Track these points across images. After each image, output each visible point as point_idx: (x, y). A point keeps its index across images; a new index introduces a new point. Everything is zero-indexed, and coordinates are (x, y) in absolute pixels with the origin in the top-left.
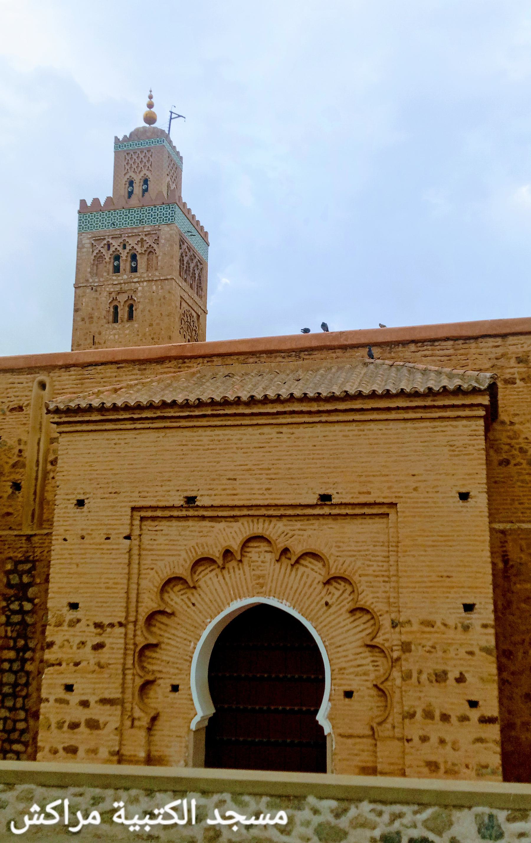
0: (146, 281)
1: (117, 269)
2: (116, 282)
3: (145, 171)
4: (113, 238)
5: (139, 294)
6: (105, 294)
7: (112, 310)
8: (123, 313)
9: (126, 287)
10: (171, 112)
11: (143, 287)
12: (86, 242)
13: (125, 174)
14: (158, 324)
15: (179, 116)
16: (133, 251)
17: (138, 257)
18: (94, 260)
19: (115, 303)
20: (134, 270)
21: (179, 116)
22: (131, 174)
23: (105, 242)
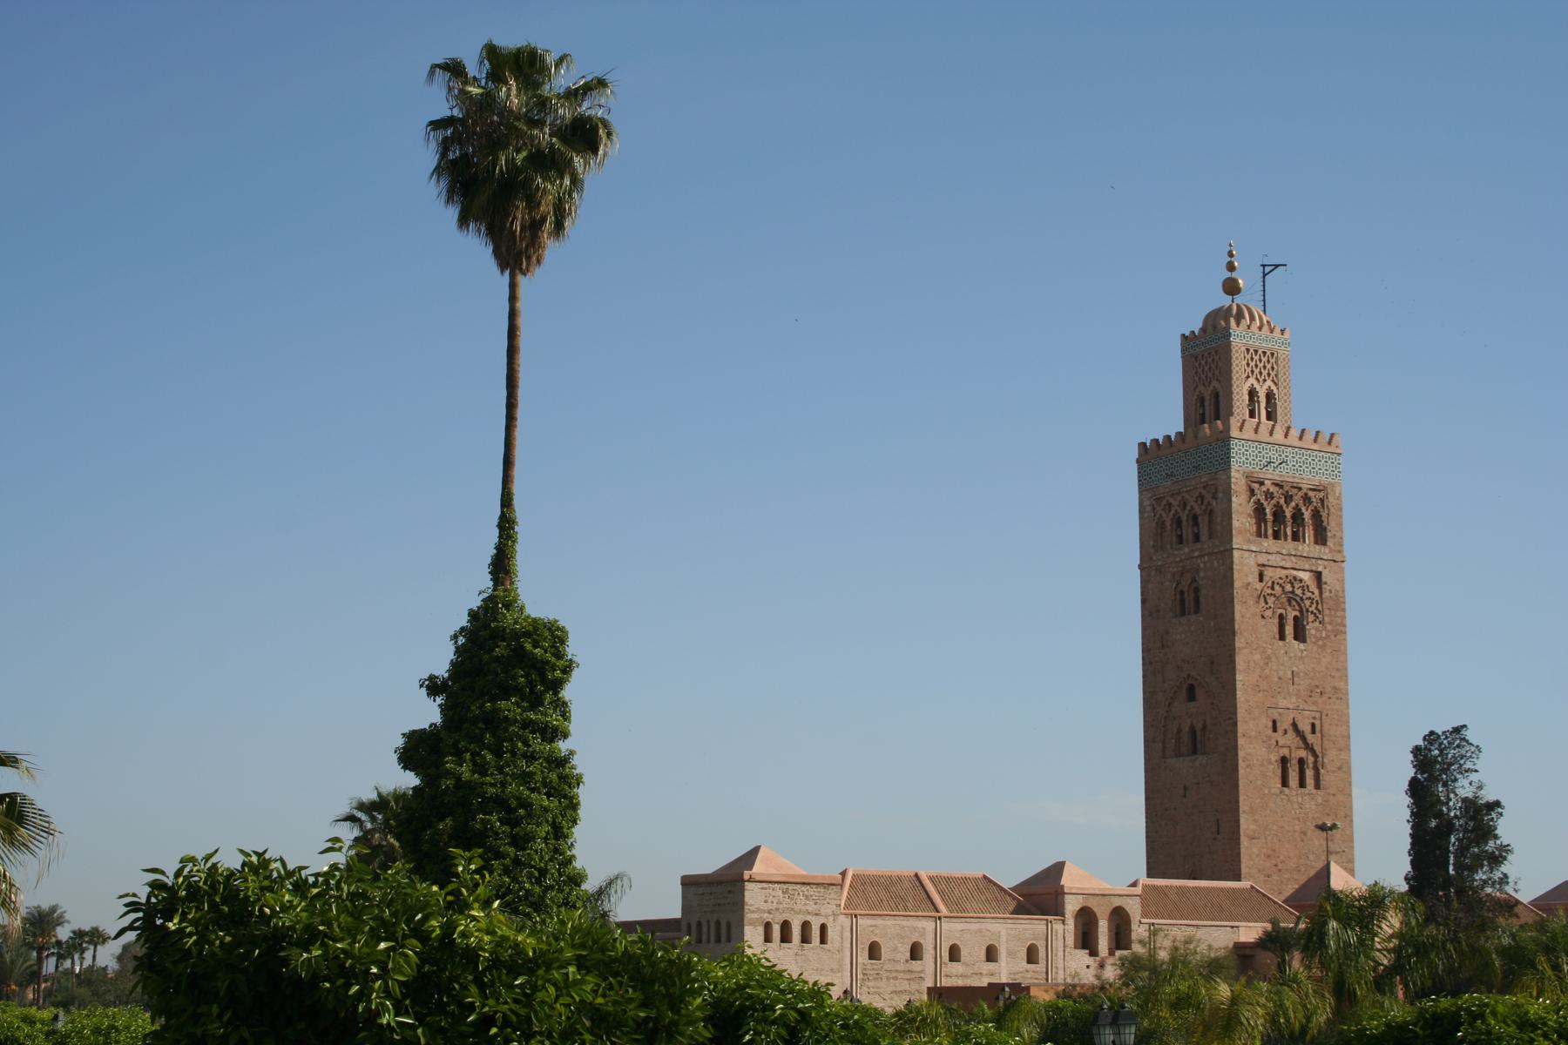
1: (1180, 539)
6: (1169, 576)
8: (1189, 603)
20: (1197, 538)
22: (1201, 388)
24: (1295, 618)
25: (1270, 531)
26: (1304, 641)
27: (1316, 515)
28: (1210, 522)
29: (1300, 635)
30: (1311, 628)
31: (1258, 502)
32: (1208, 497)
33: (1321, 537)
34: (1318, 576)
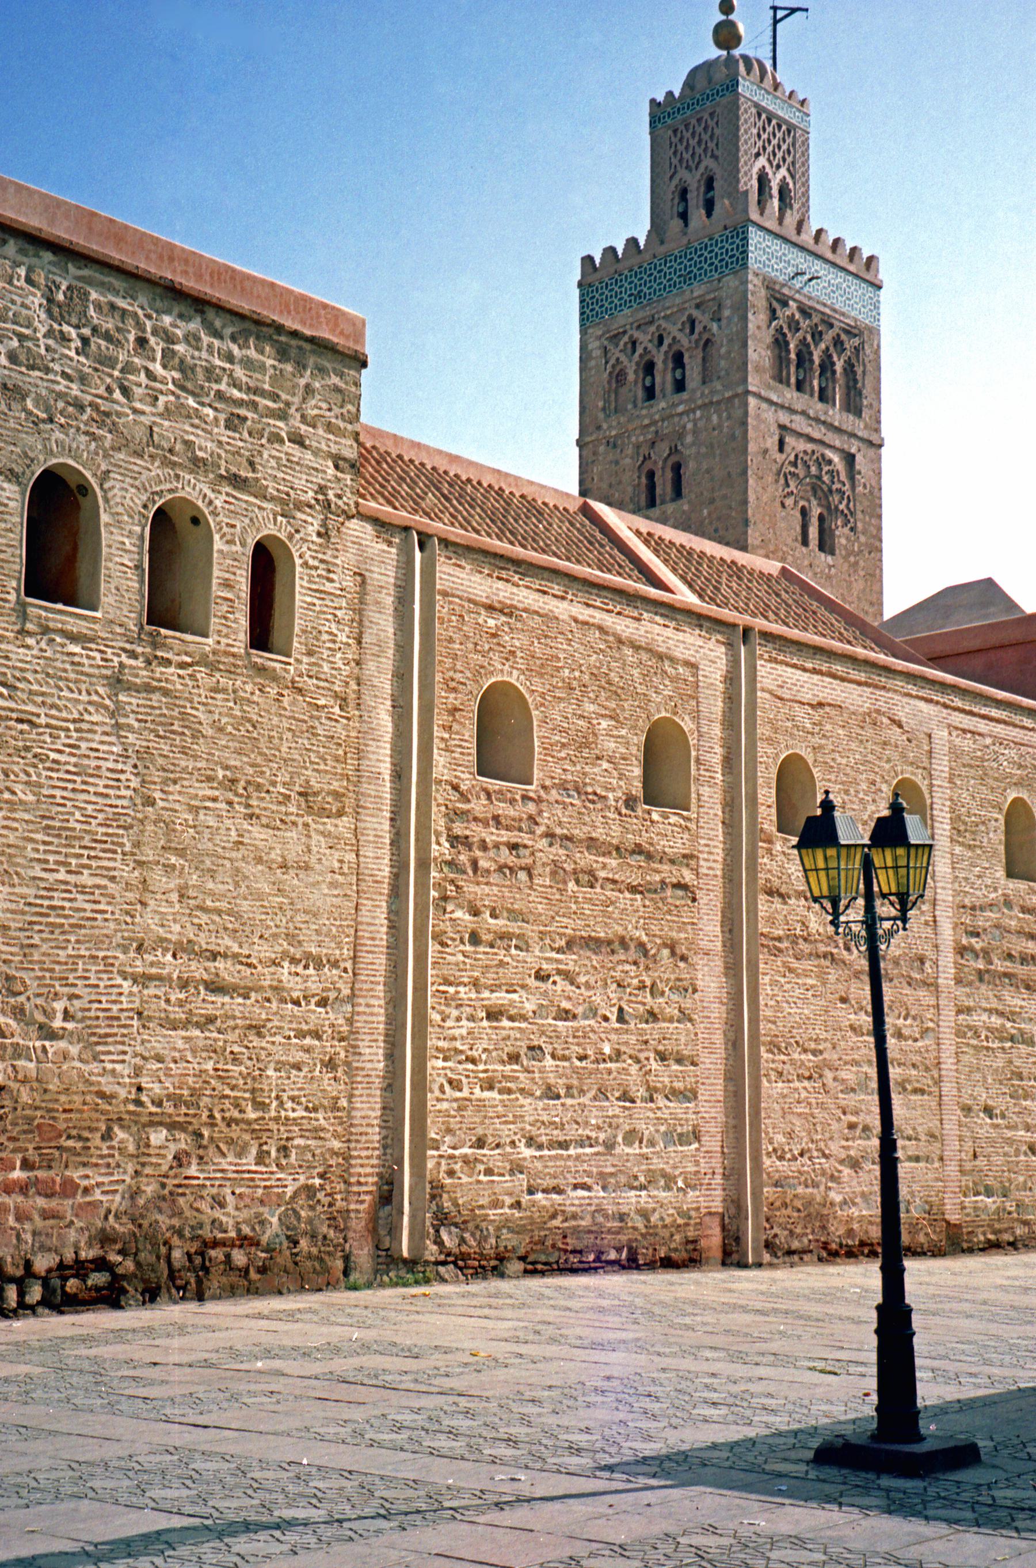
0: (700, 407)
1: (650, 393)
2: (646, 422)
3: (708, 162)
4: (639, 327)
5: (689, 439)
6: (630, 451)
7: (644, 480)
8: (664, 485)
9: (666, 428)
10: (775, 9)
11: (695, 422)
12: (594, 345)
13: (671, 177)
14: (725, 497)
15: (793, 11)
16: (675, 348)
17: (686, 359)
18: (609, 382)
19: (649, 465)
20: (680, 386)
21: (793, 11)
23: (626, 339)
24: (821, 518)
25: (793, 380)
26: (832, 553)
27: (850, 369)
28: (704, 359)
29: (826, 545)
30: (841, 535)
31: (779, 330)
32: (702, 318)
33: (853, 405)
34: (850, 459)
